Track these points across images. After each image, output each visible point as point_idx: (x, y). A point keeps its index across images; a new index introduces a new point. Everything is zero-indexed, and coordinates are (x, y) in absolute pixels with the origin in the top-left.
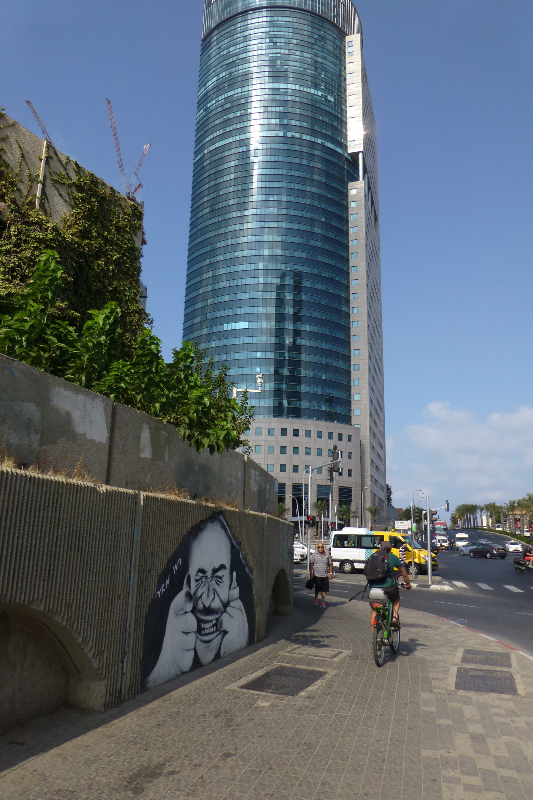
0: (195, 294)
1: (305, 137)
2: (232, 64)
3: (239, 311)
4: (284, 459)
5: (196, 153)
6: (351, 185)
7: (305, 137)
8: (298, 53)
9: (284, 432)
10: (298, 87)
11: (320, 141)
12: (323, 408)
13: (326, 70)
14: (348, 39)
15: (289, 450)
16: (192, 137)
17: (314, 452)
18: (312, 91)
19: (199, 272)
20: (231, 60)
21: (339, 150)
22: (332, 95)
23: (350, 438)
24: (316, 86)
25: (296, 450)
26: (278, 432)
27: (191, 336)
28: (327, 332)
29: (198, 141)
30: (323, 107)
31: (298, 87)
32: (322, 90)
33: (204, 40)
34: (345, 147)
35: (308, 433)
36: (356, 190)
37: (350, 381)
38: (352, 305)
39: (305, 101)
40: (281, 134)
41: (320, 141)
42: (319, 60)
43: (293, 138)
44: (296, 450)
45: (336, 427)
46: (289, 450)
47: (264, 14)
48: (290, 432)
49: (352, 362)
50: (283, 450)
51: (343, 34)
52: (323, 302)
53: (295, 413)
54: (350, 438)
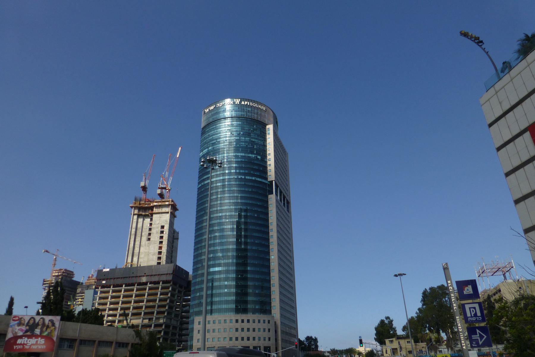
0: (199, 246)
1: (247, 177)
2: (214, 144)
3: (217, 262)
4: (237, 334)
5: (199, 183)
6: (270, 196)
7: (247, 177)
8: (243, 138)
9: (237, 321)
10: (243, 154)
11: (254, 178)
12: (257, 307)
13: (257, 144)
14: (267, 127)
15: (240, 330)
16: (197, 175)
17: (251, 330)
18: (250, 155)
19: (200, 242)
20: (214, 142)
21: (263, 181)
22: (259, 155)
23: (269, 322)
24: (252, 153)
25: (243, 330)
26: (234, 321)
27: (196, 273)
28: (258, 269)
29: (200, 177)
30: (255, 162)
31: (243, 154)
32: (254, 154)
33: (203, 129)
34: (266, 179)
35: (248, 321)
36: (272, 199)
37: (270, 293)
38: (271, 254)
39: (247, 160)
40: (236, 177)
41: (254, 178)
42: (253, 140)
43: (241, 178)
44: (243, 330)
45: (262, 317)
46: (240, 330)
47: (228, 121)
48: (240, 321)
49: (272, 283)
50: (237, 330)
51: (264, 125)
52: (256, 255)
53: (245, 311)
54: (269, 322)
